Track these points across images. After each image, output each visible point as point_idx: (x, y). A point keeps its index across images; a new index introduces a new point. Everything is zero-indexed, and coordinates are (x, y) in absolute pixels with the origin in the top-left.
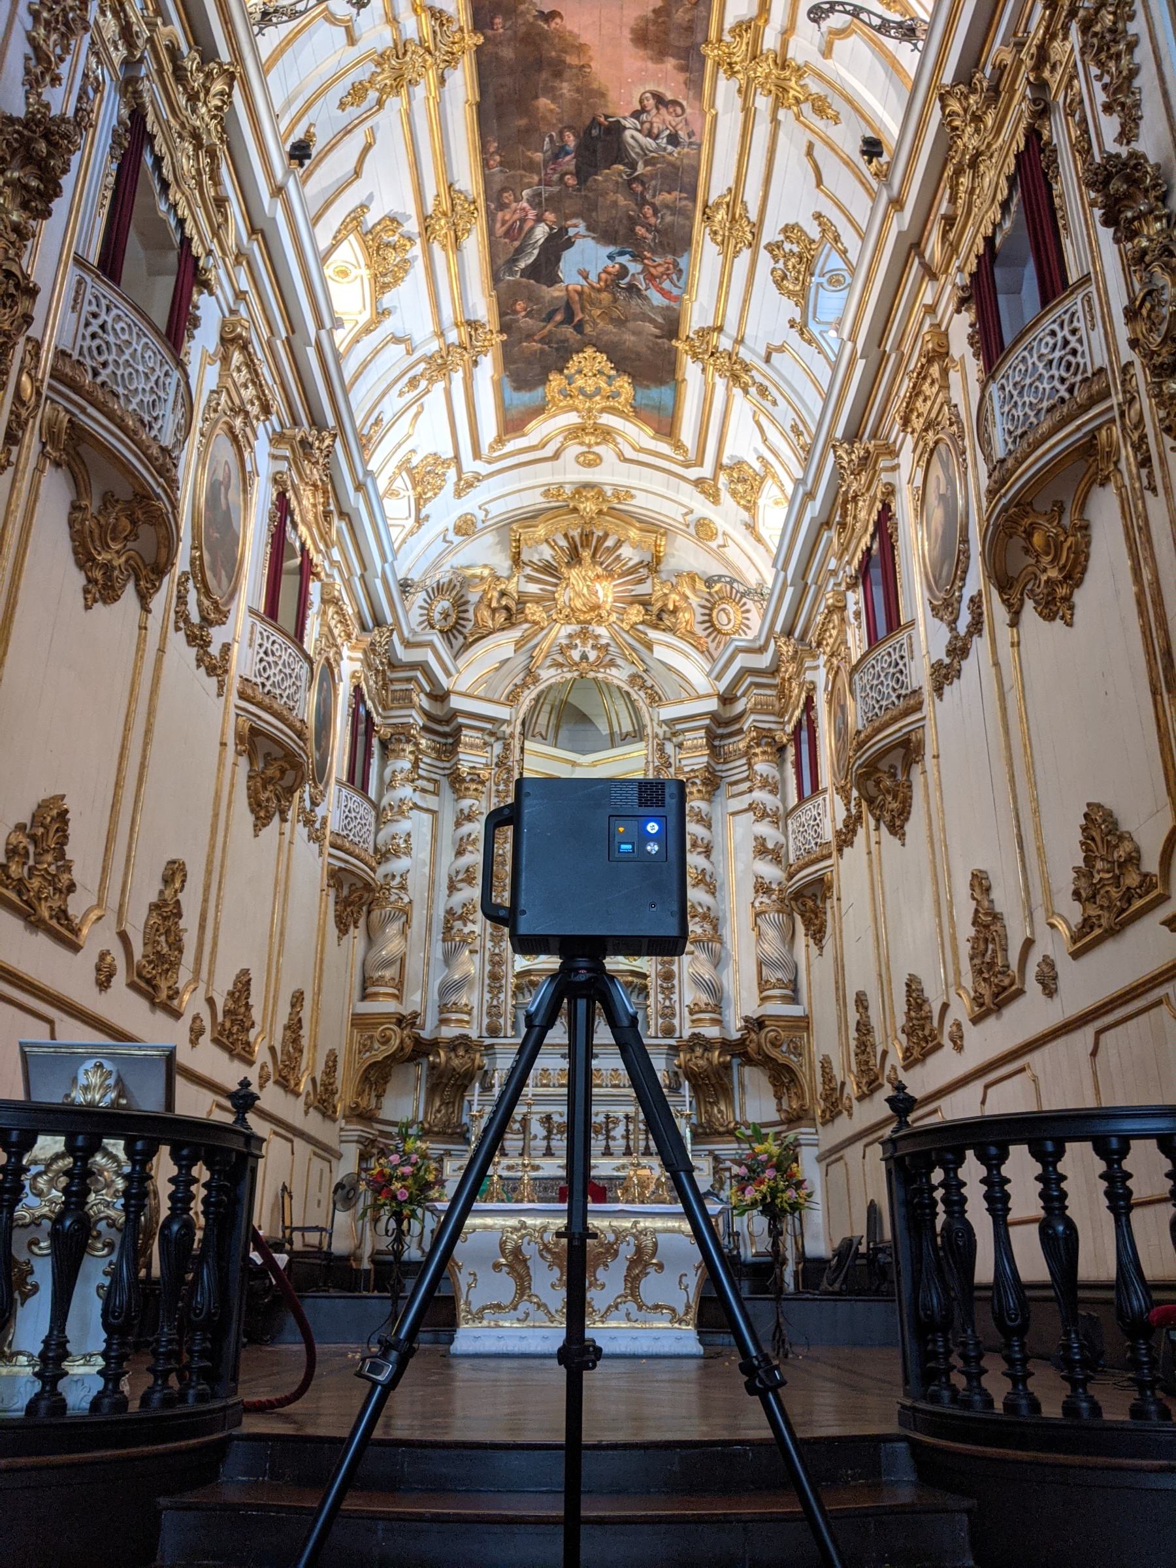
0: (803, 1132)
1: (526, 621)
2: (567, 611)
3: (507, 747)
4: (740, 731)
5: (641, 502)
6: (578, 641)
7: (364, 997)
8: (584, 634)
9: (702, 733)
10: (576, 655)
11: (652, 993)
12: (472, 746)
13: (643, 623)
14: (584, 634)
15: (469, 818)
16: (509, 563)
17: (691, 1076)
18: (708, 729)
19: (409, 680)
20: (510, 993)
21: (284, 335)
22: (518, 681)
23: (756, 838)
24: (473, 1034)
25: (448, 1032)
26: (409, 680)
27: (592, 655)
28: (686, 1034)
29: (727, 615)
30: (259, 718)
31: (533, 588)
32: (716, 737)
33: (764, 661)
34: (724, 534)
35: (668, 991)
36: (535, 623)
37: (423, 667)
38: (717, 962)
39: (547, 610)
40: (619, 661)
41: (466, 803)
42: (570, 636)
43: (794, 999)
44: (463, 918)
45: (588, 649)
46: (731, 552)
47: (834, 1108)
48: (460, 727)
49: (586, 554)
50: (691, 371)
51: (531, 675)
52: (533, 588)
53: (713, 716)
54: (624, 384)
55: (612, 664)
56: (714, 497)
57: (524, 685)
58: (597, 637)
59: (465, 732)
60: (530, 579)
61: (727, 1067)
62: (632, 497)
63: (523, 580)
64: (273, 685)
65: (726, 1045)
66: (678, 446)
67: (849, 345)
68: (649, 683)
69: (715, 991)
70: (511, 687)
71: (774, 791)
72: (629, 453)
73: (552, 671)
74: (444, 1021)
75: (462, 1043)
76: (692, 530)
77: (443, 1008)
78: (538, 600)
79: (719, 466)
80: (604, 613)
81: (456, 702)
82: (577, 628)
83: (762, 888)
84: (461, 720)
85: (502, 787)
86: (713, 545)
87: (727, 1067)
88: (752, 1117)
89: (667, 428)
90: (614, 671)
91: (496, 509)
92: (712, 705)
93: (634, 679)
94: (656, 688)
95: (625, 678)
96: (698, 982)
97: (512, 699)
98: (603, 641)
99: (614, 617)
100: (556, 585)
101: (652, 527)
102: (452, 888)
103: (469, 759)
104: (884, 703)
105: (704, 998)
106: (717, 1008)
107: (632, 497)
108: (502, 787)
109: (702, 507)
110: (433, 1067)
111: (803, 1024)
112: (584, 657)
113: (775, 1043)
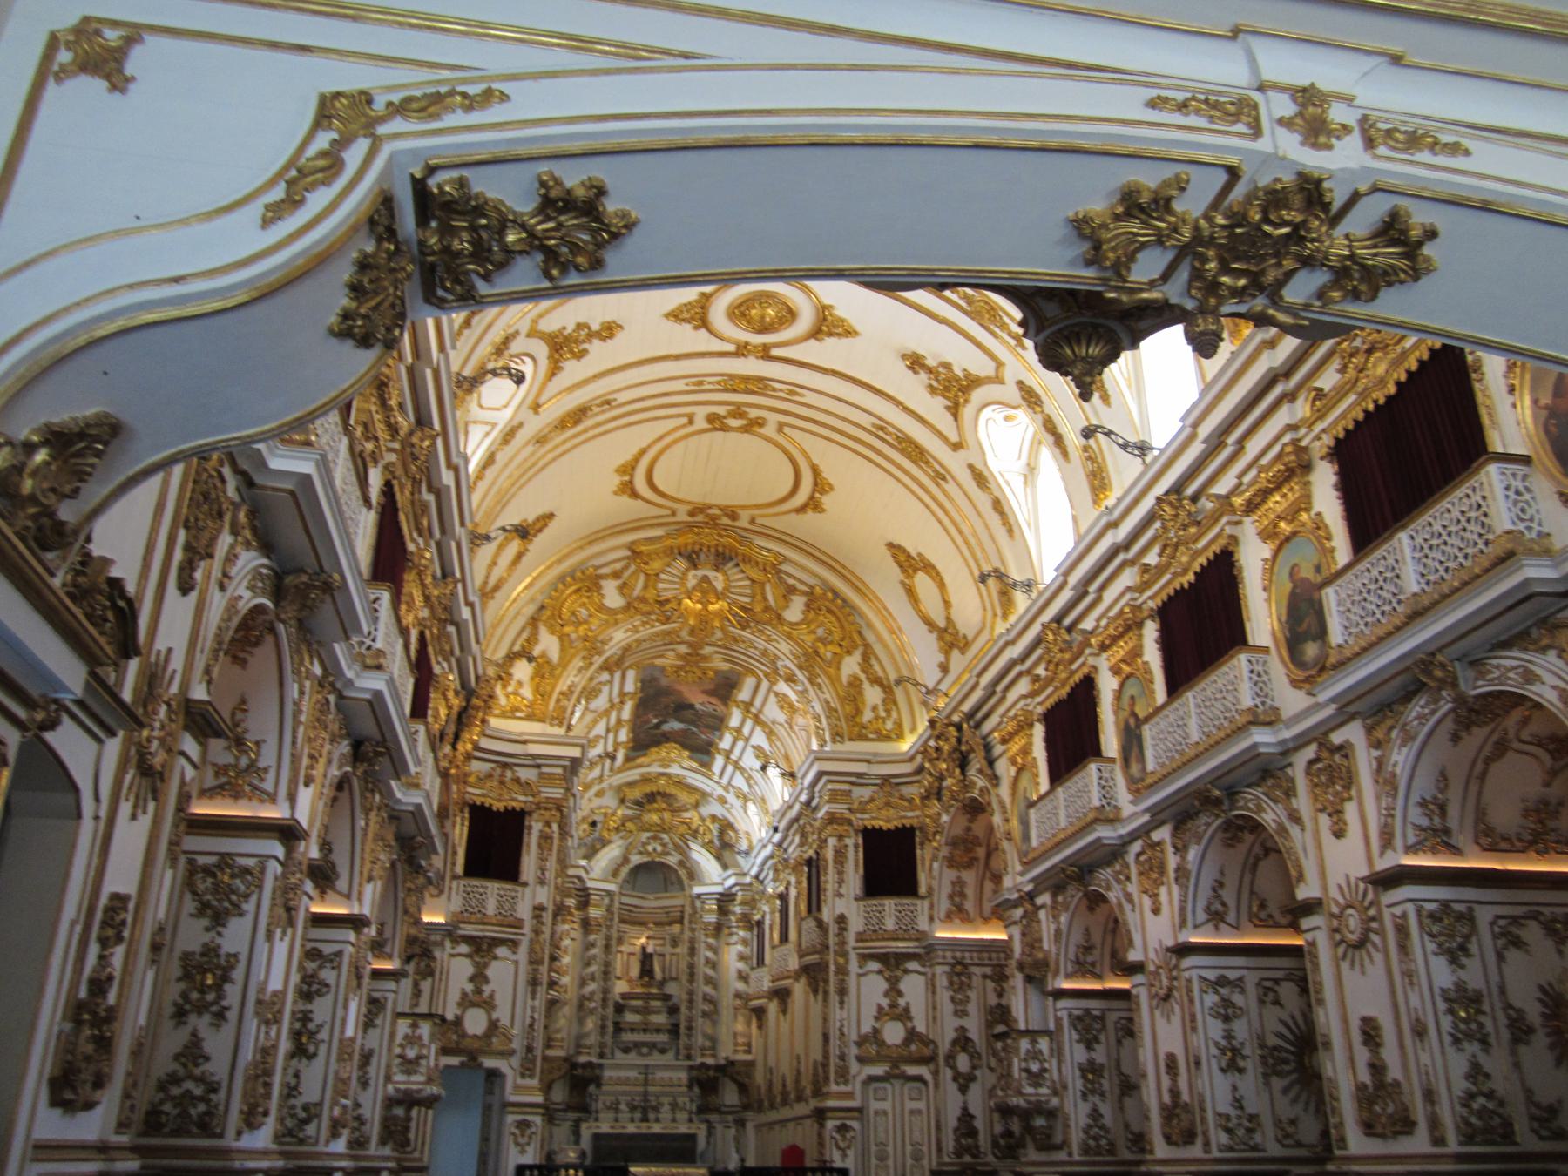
0: (749, 1115)
3: (612, 901)
5: (689, 781)
7: (548, 1046)
14: (655, 838)
15: (593, 945)
17: (701, 1084)
24: (594, 1060)
25: (582, 1059)
27: (659, 849)
28: (699, 1060)
31: (630, 812)
33: (748, 880)
35: (689, 1036)
37: (579, 878)
38: (715, 1023)
41: (592, 937)
43: (749, 1052)
44: (590, 999)
47: (760, 1109)
49: (659, 798)
50: (719, 762)
51: (626, 860)
52: (630, 812)
53: (721, 894)
54: (686, 753)
55: (668, 854)
57: (622, 865)
61: (716, 1079)
65: (719, 1068)
69: (713, 1040)
74: (579, 1053)
75: (590, 1065)
77: (578, 1046)
79: (729, 783)
81: (590, 884)
83: (738, 995)
87: (716, 1079)
88: (728, 1102)
89: (707, 765)
92: (719, 889)
93: (681, 863)
96: (706, 1036)
97: (615, 873)
101: (692, 789)
102: (583, 983)
103: (595, 913)
105: (708, 1044)
106: (713, 1048)
109: (719, 791)
110: (573, 1077)
111: (751, 1064)
113: (738, 1073)
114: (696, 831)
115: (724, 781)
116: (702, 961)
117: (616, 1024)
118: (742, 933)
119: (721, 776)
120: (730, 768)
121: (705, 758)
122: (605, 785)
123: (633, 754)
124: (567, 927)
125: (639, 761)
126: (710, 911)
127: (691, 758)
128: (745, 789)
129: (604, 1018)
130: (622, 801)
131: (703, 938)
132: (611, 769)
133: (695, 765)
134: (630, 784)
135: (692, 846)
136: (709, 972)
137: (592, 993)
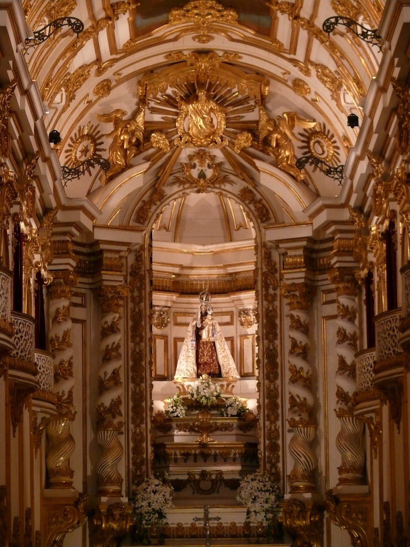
1: (152, 147)
2: (186, 138)
4: (331, 249)
5: (246, 60)
6: (196, 161)
8: (201, 155)
9: (301, 252)
10: (195, 173)
11: (262, 463)
12: (111, 268)
13: (251, 146)
15: (112, 329)
16: (136, 100)
18: (305, 249)
19: (65, 234)
20: (149, 465)
21: (17, 135)
22: (146, 198)
23: (339, 356)
26: (65, 234)
27: (209, 173)
29: (322, 147)
30: (19, 377)
31: (157, 118)
32: (313, 251)
33: (346, 215)
34: (316, 93)
36: (160, 149)
39: (168, 136)
40: (232, 178)
41: (110, 318)
42: (191, 157)
45: (205, 168)
46: (321, 105)
48: (102, 252)
49: (202, 94)
53: (309, 239)
55: (225, 180)
56: (307, 73)
57: (151, 202)
58: (213, 158)
59: (106, 255)
60: (154, 110)
62: (240, 58)
63: (148, 112)
64: (21, 352)
66: (275, 40)
67: (369, 121)
68: (258, 197)
70: (140, 204)
71: (351, 320)
72: (235, 37)
73: (176, 188)
76: (290, 83)
78: (160, 128)
80: (218, 140)
81: (100, 235)
82: (196, 149)
83: (342, 395)
84: (102, 246)
85: (136, 294)
86: (309, 97)
90: (228, 187)
91: (126, 72)
92: (307, 232)
94: (264, 202)
95: (237, 192)
98: (218, 161)
99: (226, 143)
100: (177, 114)
104: (387, 352)
107: (240, 58)
108: (136, 294)
109: (296, 73)
112: (202, 175)
114: (266, 142)
115: (300, 55)
116: (288, 345)
117: (159, 448)
118: (344, 300)
119: (293, 49)
120: (303, 34)
121: (264, 20)
122: (108, 74)
123: (142, 22)
124: (63, 303)
125: (159, 32)
126: (295, 266)
127: (240, 22)
128: (332, 66)
129: (138, 440)
130: (143, 101)
131: (286, 309)
132: (113, 49)
133: (250, 33)
134: (150, 72)
135: (258, 163)
136: (299, 363)
137: (116, 403)
